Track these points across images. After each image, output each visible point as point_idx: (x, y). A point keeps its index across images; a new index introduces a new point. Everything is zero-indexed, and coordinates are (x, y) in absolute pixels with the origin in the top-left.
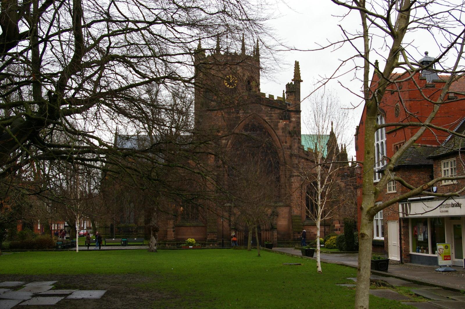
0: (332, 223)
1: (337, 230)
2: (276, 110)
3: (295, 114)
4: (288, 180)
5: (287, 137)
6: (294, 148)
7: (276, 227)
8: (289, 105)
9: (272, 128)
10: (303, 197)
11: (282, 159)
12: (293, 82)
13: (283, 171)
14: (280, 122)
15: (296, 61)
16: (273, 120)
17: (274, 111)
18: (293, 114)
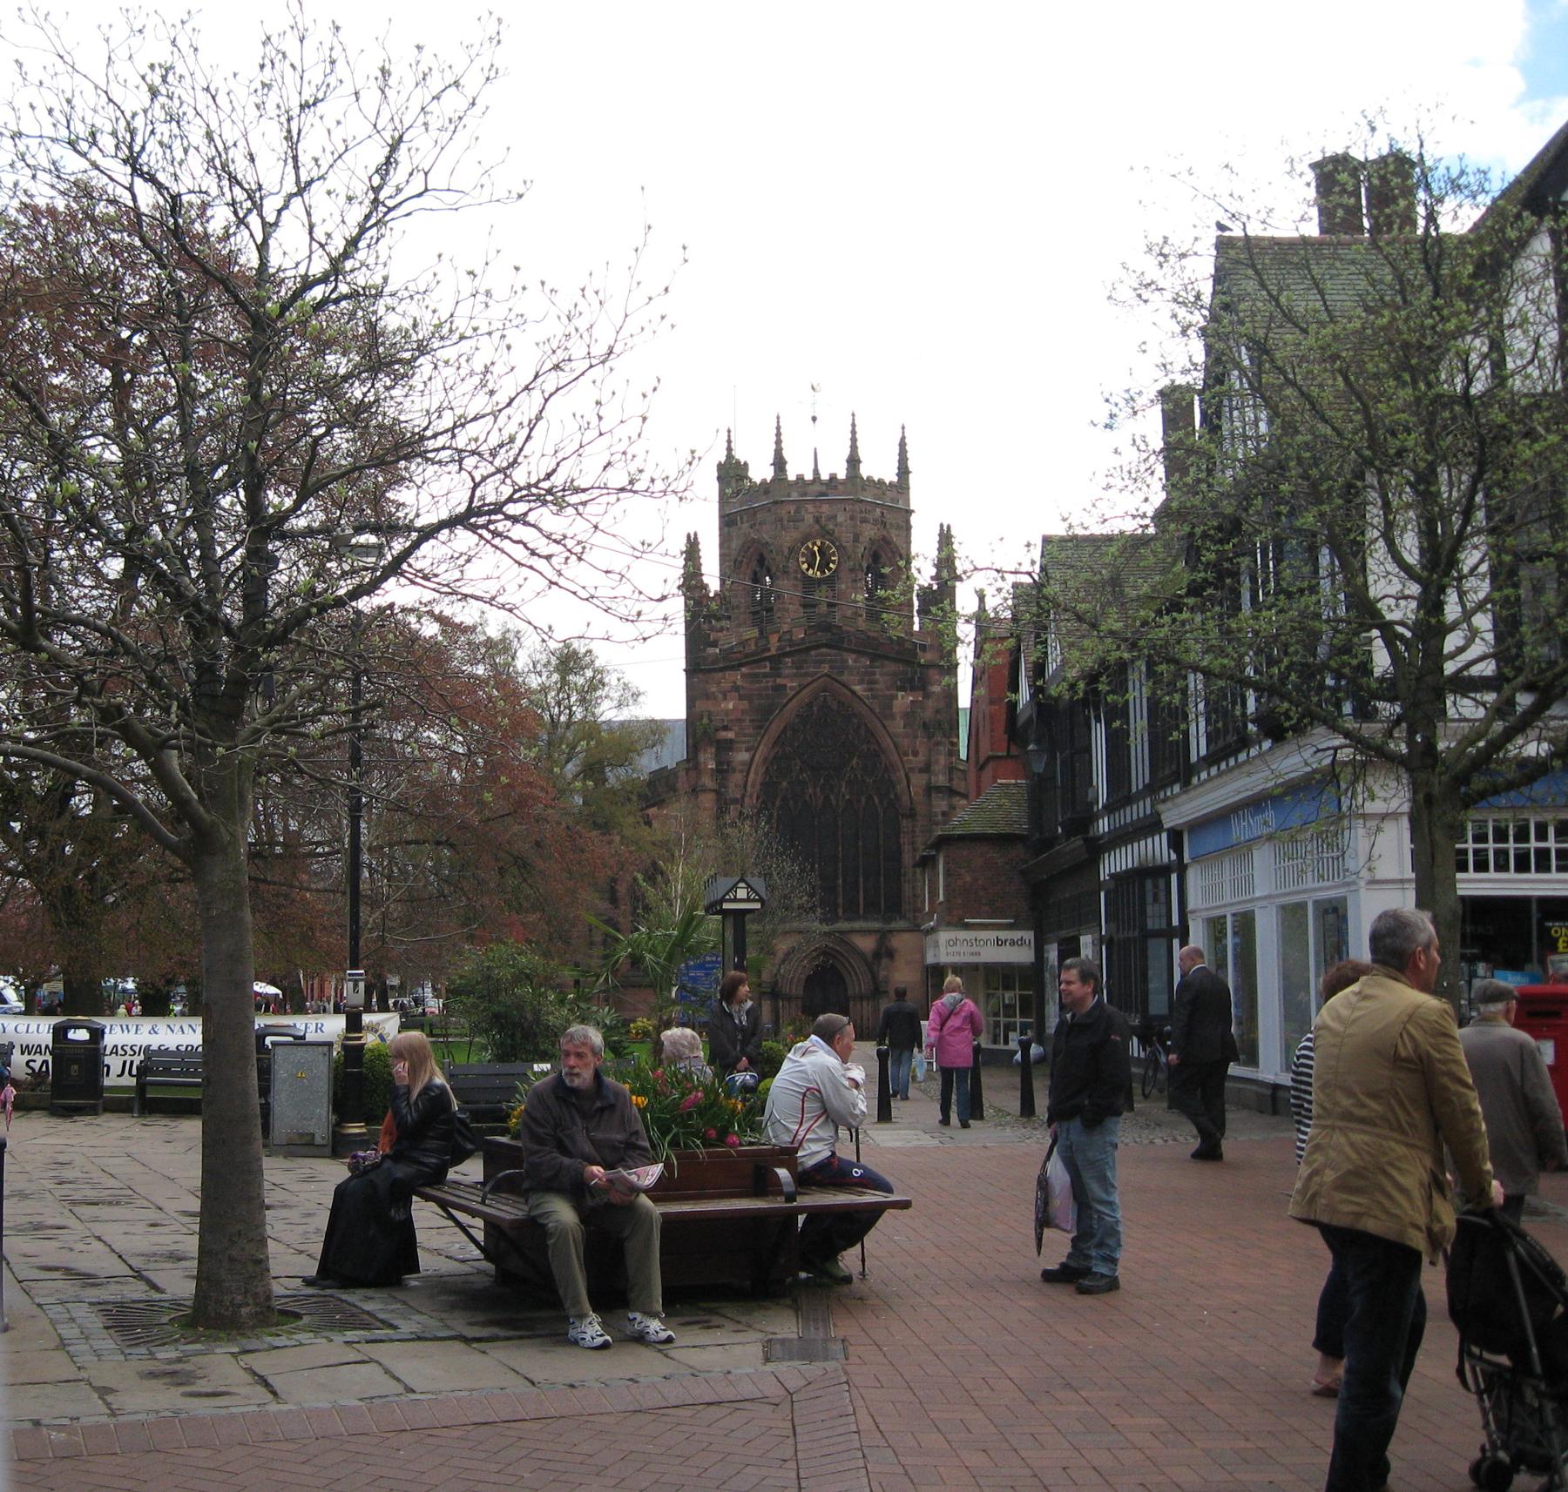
6: (936, 768)
8: (923, 648)
11: (905, 798)
18: (933, 674)
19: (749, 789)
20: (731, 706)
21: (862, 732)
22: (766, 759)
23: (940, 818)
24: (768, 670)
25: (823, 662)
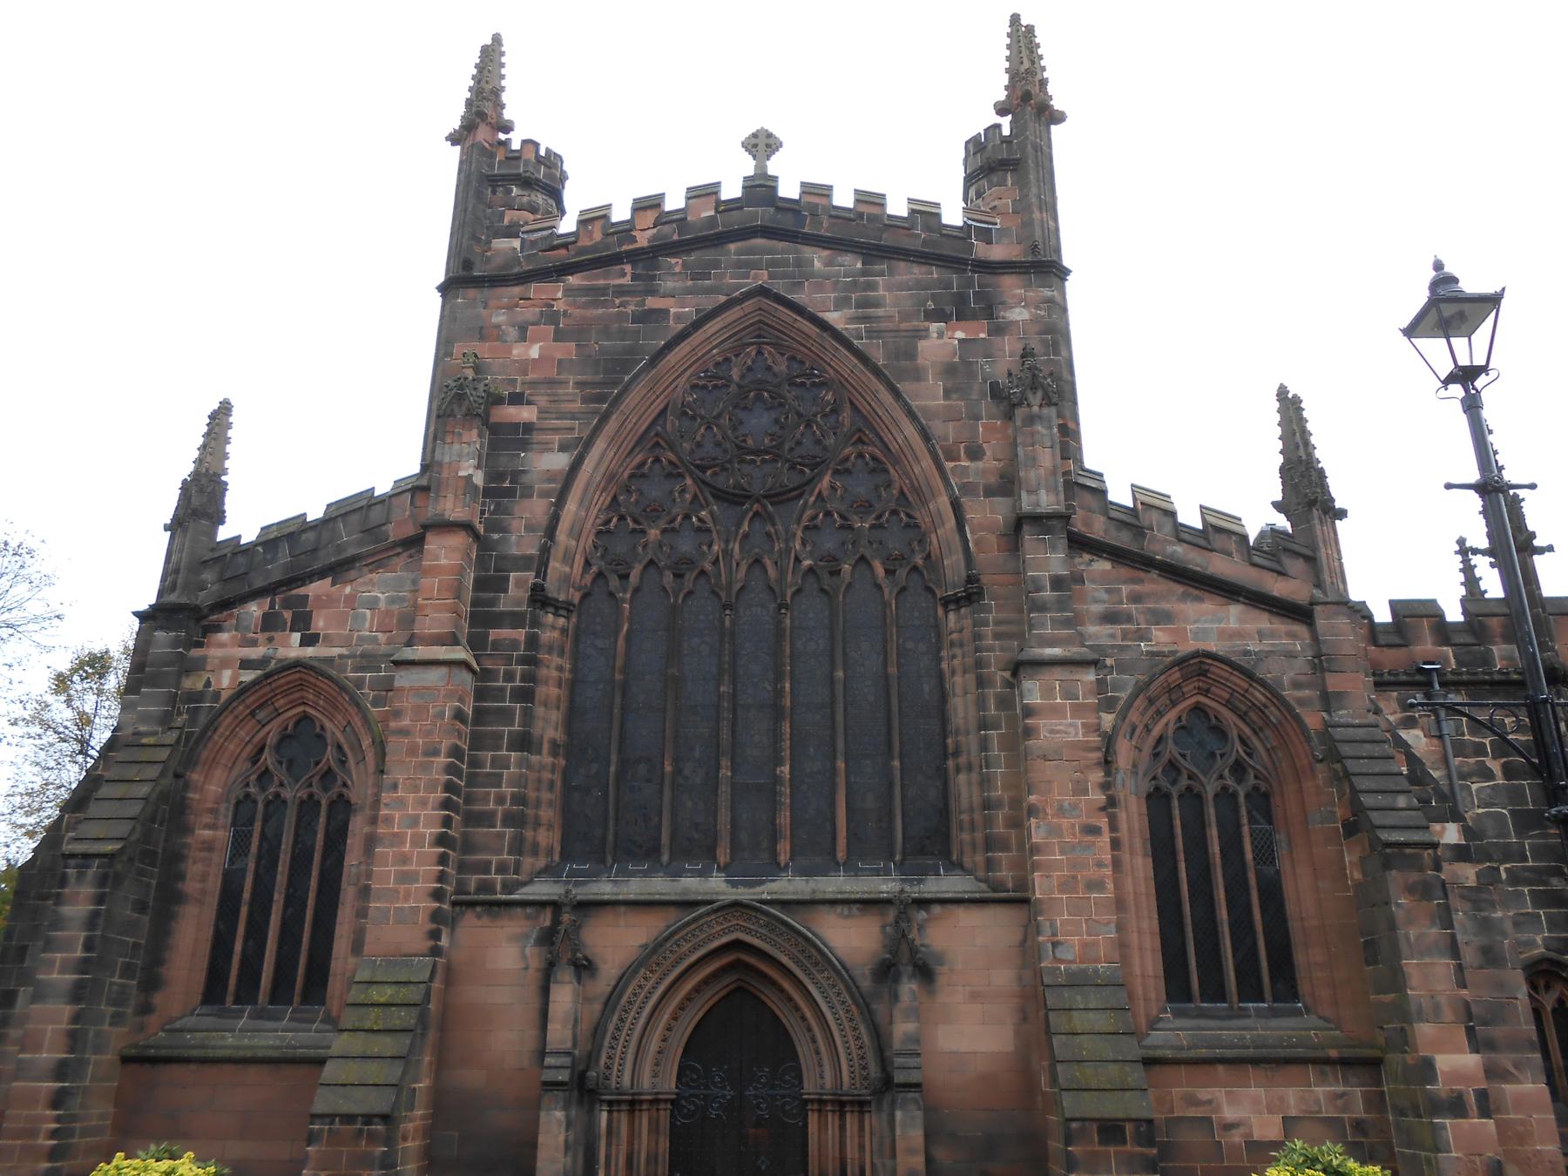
0: (1404, 1040)
1: (1456, 1107)
2: (902, 265)
3: (1028, 286)
4: (1005, 703)
5: (978, 418)
6: (1029, 475)
7: (914, 1077)
9: (877, 372)
12: (1006, 123)
13: (962, 645)
14: (927, 337)
15: (1015, 20)
16: (884, 325)
17: (891, 273)
19: (562, 536)
20: (535, 352)
21: (846, 416)
22: (611, 477)
23: (1047, 594)
24: (627, 280)
25: (755, 265)
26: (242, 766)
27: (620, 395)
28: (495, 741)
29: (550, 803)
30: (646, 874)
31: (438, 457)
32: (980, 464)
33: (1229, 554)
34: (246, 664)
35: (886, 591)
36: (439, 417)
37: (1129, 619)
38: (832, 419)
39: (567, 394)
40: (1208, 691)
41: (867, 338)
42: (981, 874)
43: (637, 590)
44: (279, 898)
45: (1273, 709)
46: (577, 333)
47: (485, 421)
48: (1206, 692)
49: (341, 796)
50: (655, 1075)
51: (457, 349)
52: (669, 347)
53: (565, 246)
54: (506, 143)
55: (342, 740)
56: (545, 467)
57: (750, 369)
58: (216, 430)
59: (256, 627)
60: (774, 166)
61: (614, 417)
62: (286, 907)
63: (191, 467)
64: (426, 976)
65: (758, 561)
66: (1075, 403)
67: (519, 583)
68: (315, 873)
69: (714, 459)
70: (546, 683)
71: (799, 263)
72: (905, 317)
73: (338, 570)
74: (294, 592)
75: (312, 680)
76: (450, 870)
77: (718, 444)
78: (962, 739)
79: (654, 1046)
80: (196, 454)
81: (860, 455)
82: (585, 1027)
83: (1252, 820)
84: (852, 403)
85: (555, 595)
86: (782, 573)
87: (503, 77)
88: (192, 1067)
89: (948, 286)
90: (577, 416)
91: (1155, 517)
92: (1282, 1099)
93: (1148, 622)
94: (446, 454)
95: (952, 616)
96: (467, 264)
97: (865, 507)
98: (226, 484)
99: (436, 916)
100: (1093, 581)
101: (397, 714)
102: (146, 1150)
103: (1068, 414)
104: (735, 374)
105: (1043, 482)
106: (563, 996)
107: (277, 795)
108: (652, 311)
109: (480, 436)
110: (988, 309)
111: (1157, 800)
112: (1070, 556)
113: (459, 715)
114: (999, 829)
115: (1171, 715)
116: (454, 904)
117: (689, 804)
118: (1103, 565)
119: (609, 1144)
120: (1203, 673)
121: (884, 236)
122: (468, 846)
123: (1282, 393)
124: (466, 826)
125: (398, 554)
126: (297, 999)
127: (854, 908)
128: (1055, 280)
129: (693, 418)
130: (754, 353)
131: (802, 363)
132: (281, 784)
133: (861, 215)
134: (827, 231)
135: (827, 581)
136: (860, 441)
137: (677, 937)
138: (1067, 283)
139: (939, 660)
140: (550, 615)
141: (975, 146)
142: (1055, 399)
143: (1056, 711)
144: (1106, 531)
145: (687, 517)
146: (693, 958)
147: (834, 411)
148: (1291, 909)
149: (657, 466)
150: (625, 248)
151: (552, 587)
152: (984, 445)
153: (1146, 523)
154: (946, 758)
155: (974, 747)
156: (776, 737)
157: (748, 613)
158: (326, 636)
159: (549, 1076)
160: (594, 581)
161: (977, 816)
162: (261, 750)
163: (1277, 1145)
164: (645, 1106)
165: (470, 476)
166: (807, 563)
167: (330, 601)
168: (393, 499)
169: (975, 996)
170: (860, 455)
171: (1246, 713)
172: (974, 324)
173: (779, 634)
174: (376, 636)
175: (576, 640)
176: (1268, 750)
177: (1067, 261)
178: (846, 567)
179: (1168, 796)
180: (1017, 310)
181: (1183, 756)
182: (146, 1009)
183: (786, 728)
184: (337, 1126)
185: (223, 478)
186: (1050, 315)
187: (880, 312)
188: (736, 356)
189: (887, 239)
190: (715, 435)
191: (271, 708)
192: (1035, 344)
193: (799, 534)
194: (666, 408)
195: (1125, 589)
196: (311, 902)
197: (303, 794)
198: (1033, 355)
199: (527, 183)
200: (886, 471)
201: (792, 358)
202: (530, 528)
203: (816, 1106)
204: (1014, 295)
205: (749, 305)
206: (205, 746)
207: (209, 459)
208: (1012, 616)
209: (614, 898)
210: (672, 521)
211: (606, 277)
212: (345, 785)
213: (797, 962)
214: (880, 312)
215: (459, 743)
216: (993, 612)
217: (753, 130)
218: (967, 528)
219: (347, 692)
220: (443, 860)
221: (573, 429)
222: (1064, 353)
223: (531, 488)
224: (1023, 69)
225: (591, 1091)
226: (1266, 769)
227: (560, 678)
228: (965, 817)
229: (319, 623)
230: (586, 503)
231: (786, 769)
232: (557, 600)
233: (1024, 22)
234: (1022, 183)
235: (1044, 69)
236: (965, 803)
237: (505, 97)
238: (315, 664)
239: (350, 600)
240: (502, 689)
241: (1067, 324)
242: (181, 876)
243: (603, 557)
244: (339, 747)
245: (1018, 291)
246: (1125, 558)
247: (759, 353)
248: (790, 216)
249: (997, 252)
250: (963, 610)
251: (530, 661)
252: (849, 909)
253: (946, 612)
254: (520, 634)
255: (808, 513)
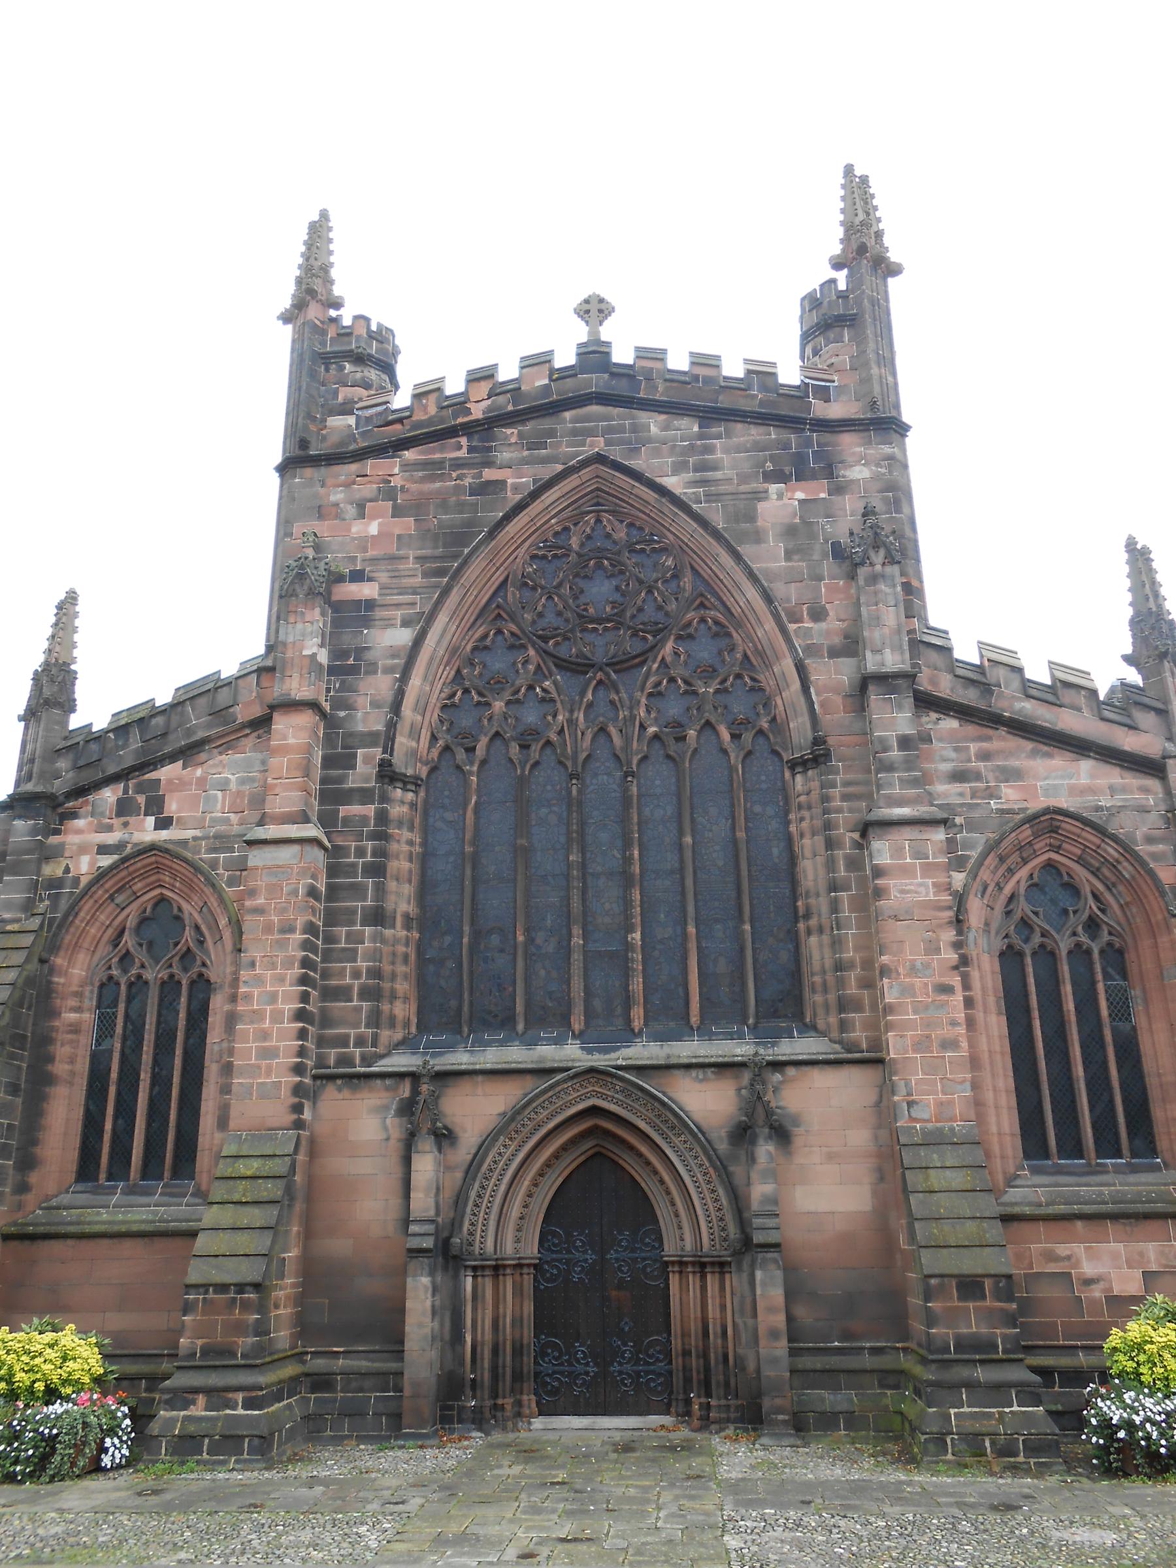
2: (739, 426)
4: (854, 864)
6: (873, 635)
7: (773, 1237)
9: (716, 534)
10: (976, 984)
12: (842, 278)
13: (809, 808)
14: (766, 498)
15: (849, 170)
16: (723, 488)
17: (728, 435)
19: (407, 710)
21: (687, 581)
22: (453, 651)
23: (895, 754)
24: (463, 453)
25: (592, 433)
26: (104, 949)
27: (459, 570)
28: (348, 917)
29: (406, 977)
30: (502, 1043)
31: (281, 637)
32: (823, 625)
33: (1079, 709)
34: (103, 850)
35: (732, 756)
36: (281, 597)
37: (978, 777)
38: (673, 584)
39: (411, 569)
40: (1059, 847)
41: (706, 502)
42: (835, 1034)
43: (483, 762)
44: (145, 1077)
45: (1126, 864)
46: (415, 508)
47: (328, 601)
48: (1057, 849)
49: (201, 975)
50: (518, 1241)
51: (297, 529)
52: (508, 518)
53: (400, 421)
54: (334, 320)
55: (200, 921)
56: (389, 644)
57: (589, 537)
58: (64, 620)
59: (111, 812)
60: (607, 332)
61: (455, 590)
62: (153, 1085)
63: (41, 658)
64: (290, 1149)
65: (603, 730)
66: (918, 560)
67: (367, 760)
68: (179, 1051)
69: (556, 629)
70: (397, 858)
71: (635, 429)
72: (744, 479)
73: (189, 752)
74: (147, 776)
75: (169, 863)
76: (310, 1045)
77: (559, 614)
78: (812, 901)
79: (515, 1211)
80: (46, 645)
81: (703, 620)
82: (448, 1195)
83: (1106, 976)
84: (692, 568)
85: (403, 771)
86: (628, 741)
87: (331, 253)
88: (70, 1242)
89: (786, 446)
90: (419, 590)
91: (1001, 674)
92: (1141, 1254)
93: (997, 780)
94: (290, 634)
95: (799, 778)
96: (304, 444)
97: (709, 672)
98: (76, 672)
99: (298, 1090)
100: (940, 740)
101: (252, 893)
102: (29, 1323)
103: (911, 571)
104: (575, 542)
105: (887, 641)
106: (425, 1165)
107: (139, 977)
108: (489, 483)
109: (323, 614)
110: (828, 469)
111: (1010, 957)
112: (917, 715)
113: (312, 892)
114: (852, 990)
115: (1023, 873)
116: (315, 1078)
117: (542, 973)
118: (951, 724)
119: (474, 1309)
120: (1054, 830)
121: (721, 398)
122: (326, 1020)
123: (1131, 545)
124: (323, 1001)
125: (247, 735)
126: (167, 1174)
127: (709, 1072)
128: (895, 436)
129: (534, 589)
130: (592, 521)
131: (641, 529)
132: (143, 966)
133: (696, 378)
134: (661, 395)
135: (673, 748)
136: (702, 605)
137: (534, 1105)
138: (907, 440)
139: (788, 823)
140: (399, 790)
141: (811, 303)
142: (898, 557)
143: (906, 871)
144: (952, 690)
145: (531, 688)
146: (551, 1125)
147: (674, 576)
148: (1148, 1065)
149: (500, 638)
150: (460, 420)
151: (399, 761)
152: (827, 606)
153: (993, 681)
154: (797, 921)
155: (825, 909)
156: (627, 903)
157: (594, 781)
158: (179, 819)
159: (414, 1243)
160: (441, 754)
161: (830, 978)
162: (122, 933)
163: (1137, 1300)
164: (508, 1271)
165: (314, 655)
166: (652, 730)
167: (182, 785)
168: (240, 681)
169: (831, 1157)
170: (703, 620)
171: (1098, 869)
172: (813, 484)
173: (626, 801)
174: (228, 818)
175: (426, 814)
176: (1121, 906)
177: (906, 417)
178: (692, 733)
179: (1021, 954)
180: (857, 468)
181: (1036, 913)
182: (23, 1188)
183: (636, 895)
184: (211, 1295)
185: (73, 667)
186: (890, 472)
187: (718, 475)
188: (575, 525)
189: (724, 401)
190: (556, 605)
191: (129, 892)
192: (877, 503)
193: (644, 701)
194: (508, 576)
195: (973, 747)
196: (176, 1080)
197: (164, 974)
198: (874, 514)
199: (360, 359)
200: (729, 635)
201: (631, 525)
202: (375, 704)
203: (676, 1268)
204: (854, 454)
205: (586, 473)
206: (67, 931)
207: (58, 649)
208: (860, 777)
209: (471, 1067)
210: (517, 691)
211: (442, 450)
212: (204, 964)
213: (654, 1127)
214: (718, 475)
215: (314, 920)
216: (841, 774)
217: (586, 296)
218: (812, 690)
219: (202, 873)
220: (302, 1034)
221: (414, 604)
222: (906, 510)
223: (375, 664)
224: (857, 221)
225: (455, 1257)
226: (1119, 924)
227: (411, 853)
228: (817, 979)
229: (172, 807)
230: (431, 678)
231: (637, 936)
232: (405, 776)
233: (858, 173)
234: (859, 340)
235: (879, 220)
236: (816, 966)
237: (334, 273)
238: (170, 847)
239: (202, 782)
240: (354, 865)
241: (909, 481)
242: (51, 1059)
243: (448, 730)
244: (197, 928)
245: (858, 449)
246: (971, 715)
247: (598, 521)
248: (624, 382)
249: (835, 410)
250: (810, 773)
251: (381, 836)
252: (705, 1073)
253: (793, 775)
254: (370, 810)
255: (652, 679)
